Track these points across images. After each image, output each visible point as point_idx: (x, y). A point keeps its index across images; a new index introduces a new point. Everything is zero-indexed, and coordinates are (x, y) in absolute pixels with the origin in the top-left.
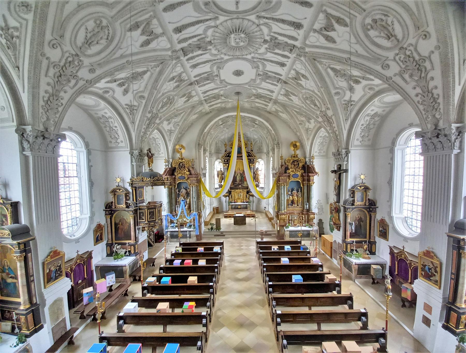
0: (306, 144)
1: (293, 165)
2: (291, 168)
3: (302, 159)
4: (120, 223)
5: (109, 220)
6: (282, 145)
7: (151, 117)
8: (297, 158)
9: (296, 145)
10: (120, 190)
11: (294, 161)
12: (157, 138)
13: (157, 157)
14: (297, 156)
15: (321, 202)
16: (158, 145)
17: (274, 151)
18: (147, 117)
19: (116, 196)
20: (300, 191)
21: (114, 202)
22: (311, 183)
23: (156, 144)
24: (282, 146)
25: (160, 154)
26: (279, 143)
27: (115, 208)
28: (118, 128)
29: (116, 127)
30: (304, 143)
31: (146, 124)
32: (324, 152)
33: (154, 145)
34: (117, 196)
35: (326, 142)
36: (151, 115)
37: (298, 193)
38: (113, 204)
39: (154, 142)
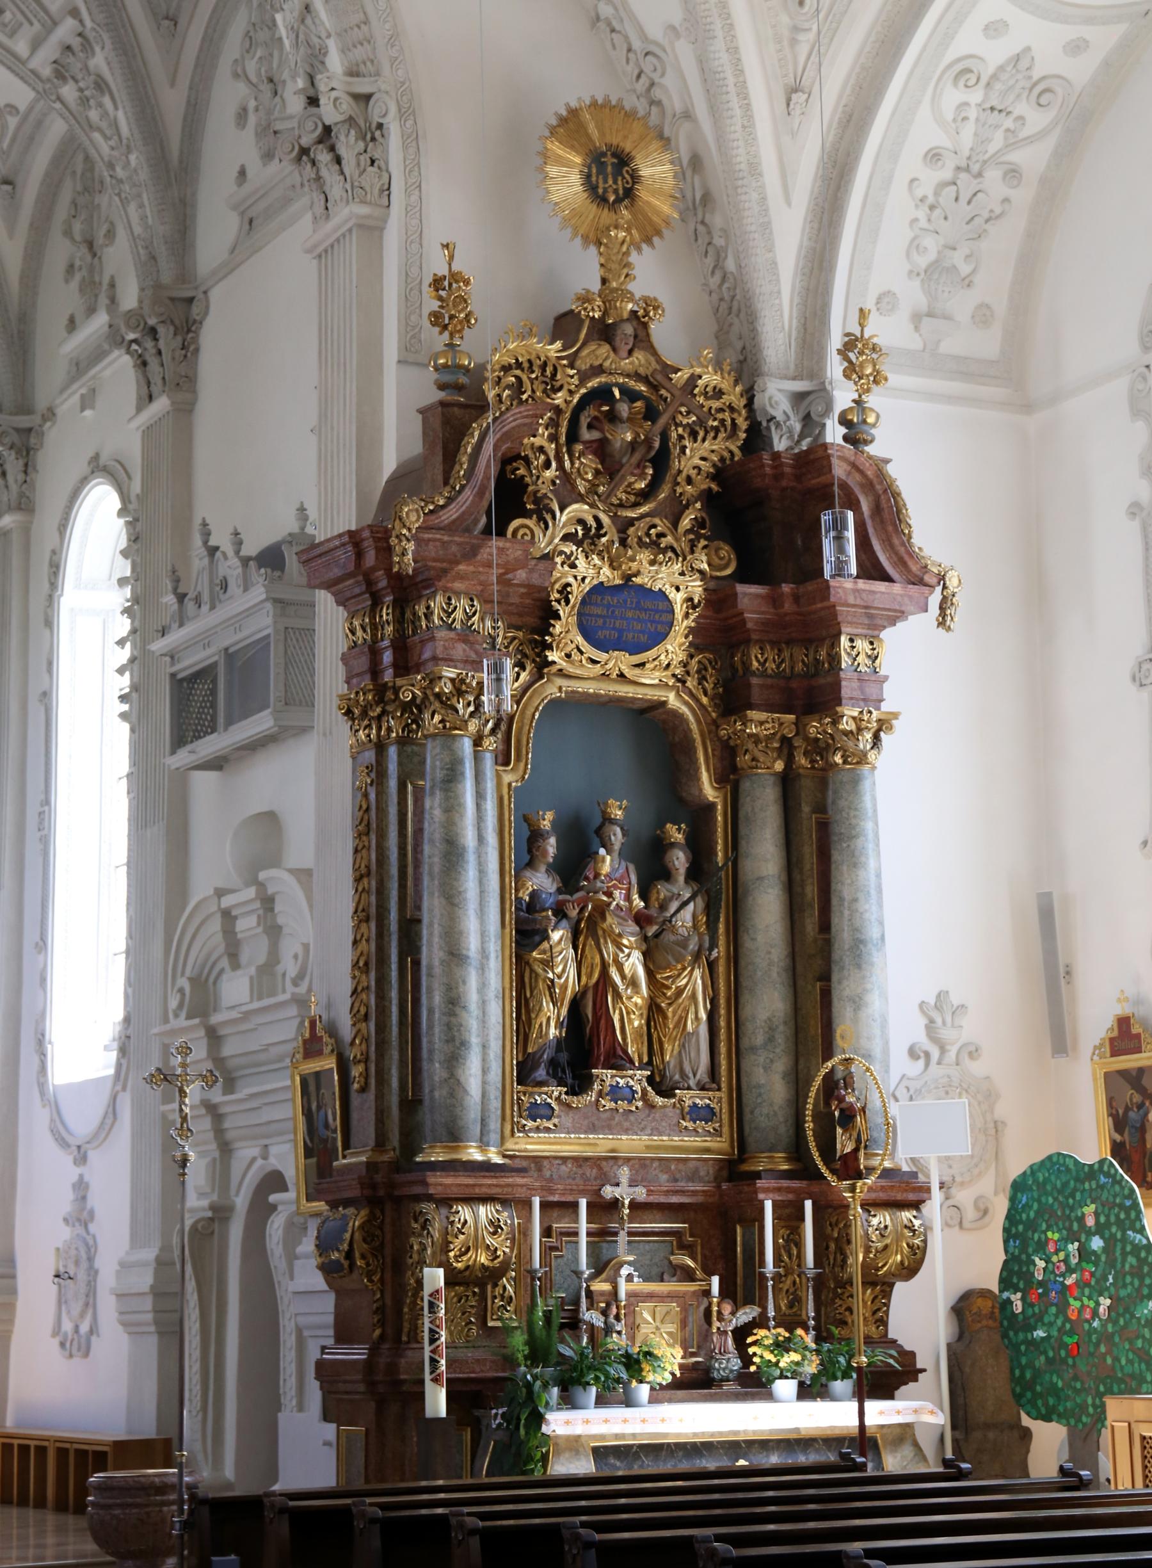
0: (755, 169)
1: (589, 462)
2: (567, 493)
3: (710, 378)
6: (413, 139)
8: (639, 357)
9: (623, 160)
11: (602, 394)
14: (640, 321)
15: (969, 1029)
17: (189, 348)
20: (679, 860)
22: (849, 712)
24: (414, 167)
26: (386, 109)
30: (741, 156)
32: (983, 315)
35: (1013, 174)
37: (662, 890)
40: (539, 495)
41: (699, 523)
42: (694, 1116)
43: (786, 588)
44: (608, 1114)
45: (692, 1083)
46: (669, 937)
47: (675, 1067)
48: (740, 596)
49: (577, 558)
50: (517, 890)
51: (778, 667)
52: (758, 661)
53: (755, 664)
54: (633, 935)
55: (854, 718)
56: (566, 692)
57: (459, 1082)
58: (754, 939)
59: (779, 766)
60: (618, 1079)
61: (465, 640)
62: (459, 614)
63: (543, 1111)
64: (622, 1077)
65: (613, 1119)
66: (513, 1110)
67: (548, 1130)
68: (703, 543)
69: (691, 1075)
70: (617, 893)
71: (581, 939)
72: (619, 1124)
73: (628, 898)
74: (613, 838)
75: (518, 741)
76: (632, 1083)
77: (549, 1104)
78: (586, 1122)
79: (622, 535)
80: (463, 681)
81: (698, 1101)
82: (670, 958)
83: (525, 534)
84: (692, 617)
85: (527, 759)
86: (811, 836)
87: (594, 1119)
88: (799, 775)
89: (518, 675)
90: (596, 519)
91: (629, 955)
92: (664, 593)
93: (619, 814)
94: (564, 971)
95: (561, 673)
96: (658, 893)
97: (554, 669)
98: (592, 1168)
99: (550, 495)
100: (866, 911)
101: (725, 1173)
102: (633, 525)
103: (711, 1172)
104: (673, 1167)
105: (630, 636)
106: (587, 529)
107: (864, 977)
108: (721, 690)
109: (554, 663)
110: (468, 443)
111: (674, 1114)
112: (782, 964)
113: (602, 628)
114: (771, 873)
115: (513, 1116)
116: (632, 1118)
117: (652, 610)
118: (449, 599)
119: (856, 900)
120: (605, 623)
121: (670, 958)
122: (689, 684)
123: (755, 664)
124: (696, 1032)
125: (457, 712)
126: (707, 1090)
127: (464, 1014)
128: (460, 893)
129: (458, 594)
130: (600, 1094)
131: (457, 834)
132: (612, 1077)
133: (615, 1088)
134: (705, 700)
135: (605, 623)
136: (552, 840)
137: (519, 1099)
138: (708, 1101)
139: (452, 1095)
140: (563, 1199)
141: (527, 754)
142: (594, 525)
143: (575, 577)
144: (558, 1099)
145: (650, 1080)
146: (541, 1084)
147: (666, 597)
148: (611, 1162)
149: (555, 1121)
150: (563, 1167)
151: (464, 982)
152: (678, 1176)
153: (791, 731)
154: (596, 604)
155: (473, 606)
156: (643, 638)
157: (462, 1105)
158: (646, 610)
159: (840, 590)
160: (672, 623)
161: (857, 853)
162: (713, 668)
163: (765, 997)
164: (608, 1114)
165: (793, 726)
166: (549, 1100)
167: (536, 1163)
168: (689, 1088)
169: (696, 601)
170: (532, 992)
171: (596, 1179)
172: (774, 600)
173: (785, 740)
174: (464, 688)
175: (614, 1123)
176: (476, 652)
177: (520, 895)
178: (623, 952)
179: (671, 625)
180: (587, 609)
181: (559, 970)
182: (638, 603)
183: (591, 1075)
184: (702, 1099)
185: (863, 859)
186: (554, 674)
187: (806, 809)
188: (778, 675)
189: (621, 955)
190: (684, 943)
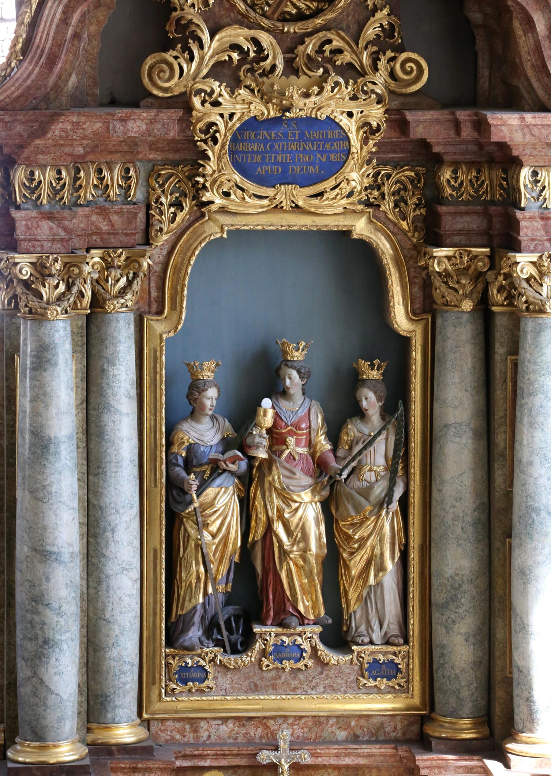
40: (183, 22)
41: (389, 31)
42: (374, 673)
43: (462, 115)
44: (273, 673)
45: (377, 636)
46: (356, 483)
47: (361, 617)
48: (412, 125)
49: (221, 95)
50: (169, 444)
51: (476, 191)
52: (453, 188)
53: (449, 191)
54: (304, 488)
55: (533, 263)
56: (229, 232)
57: (42, 682)
58: (440, 491)
59: (467, 305)
60: (285, 638)
61: (50, 216)
62: (45, 190)
63: (194, 675)
64: (289, 636)
65: (280, 677)
66: (161, 675)
67: (201, 692)
68: (390, 54)
69: (376, 627)
70: (291, 440)
71: (252, 489)
72: (286, 683)
73: (310, 444)
74: (288, 382)
75: (174, 288)
76: (299, 640)
77: (203, 667)
78: (247, 682)
79: (289, 55)
80: (44, 266)
81: (381, 658)
82: (350, 507)
83: (163, 71)
84: (371, 142)
85: (182, 307)
86: (505, 380)
87: (255, 679)
88: (493, 313)
89: (175, 215)
90: (256, 42)
91: (297, 510)
92: (333, 121)
93: (297, 356)
94: (219, 529)
95: (223, 210)
96: (347, 434)
97: (213, 207)
98: (257, 727)
99: (195, 21)
100: (541, 476)
101: (415, 728)
102: (303, 43)
103: (399, 727)
104: (353, 723)
105: (297, 169)
106: (243, 53)
107: (535, 549)
108: (423, 211)
109: (212, 202)
110: (27, 12)
111: (352, 673)
112: (469, 519)
113: (261, 164)
114: (458, 420)
115: (161, 681)
116: (301, 676)
117: (320, 140)
118: (32, 173)
119: (531, 463)
120: (263, 158)
121: (350, 507)
122: (383, 208)
123: (449, 191)
124: (379, 584)
125: (41, 297)
126: (393, 644)
127: (48, 612)
128: (45, 487)
129: (43, 167)
130: (264, 653)
131: (42, 426)
132: (277, 635)
133: (280, 648)
134: (404, 224)
135: (263, 158)
136: (212, 393)
137: (168, 665)
138: (391, 657)
139: (35, 693)
140: (216, 764)
141: (182, 301)
142: (253, 48)
143: (222, 115)
144: (213, 660)
145: (323, 637)
146: (190, 649)
147: (338, 124)
148: (280, 721)
149: (209, 682)
150: (223, 728)
151: (48, 579)
152: (359, 732)
153: (484, 265)
154: (250, 141)
155: (60, 179)
156: (315, 170)
157: (45, 705)
158: (312, 142)
159: (503, 128)
160: (349, 150)
161: (534, 412)
162: (415, 187)
163: (448, 554)
164: (273, 673)
165: (486, 260)
166: (202, 663)
167: (192, 725)
168: (372, 643)
169: (374, 124)
170: (184, 552)
171: (261, 738)
172: (457, 125)
173: (479, 276)
174: (47, 272)
175: (278, 682)
176: (65, 229)
177: (175, 449)
178: (289, 506)
179: (348, 152)
180: (240, 147)
181: (214, 528)
182: (302, 135)
183: (255, 634)
184: (385, 653)
185: (540, 419)
186: (216, 212)
187: (500, 350)
188: (476, 199)
189: (287, 510)
190: (366, 493)
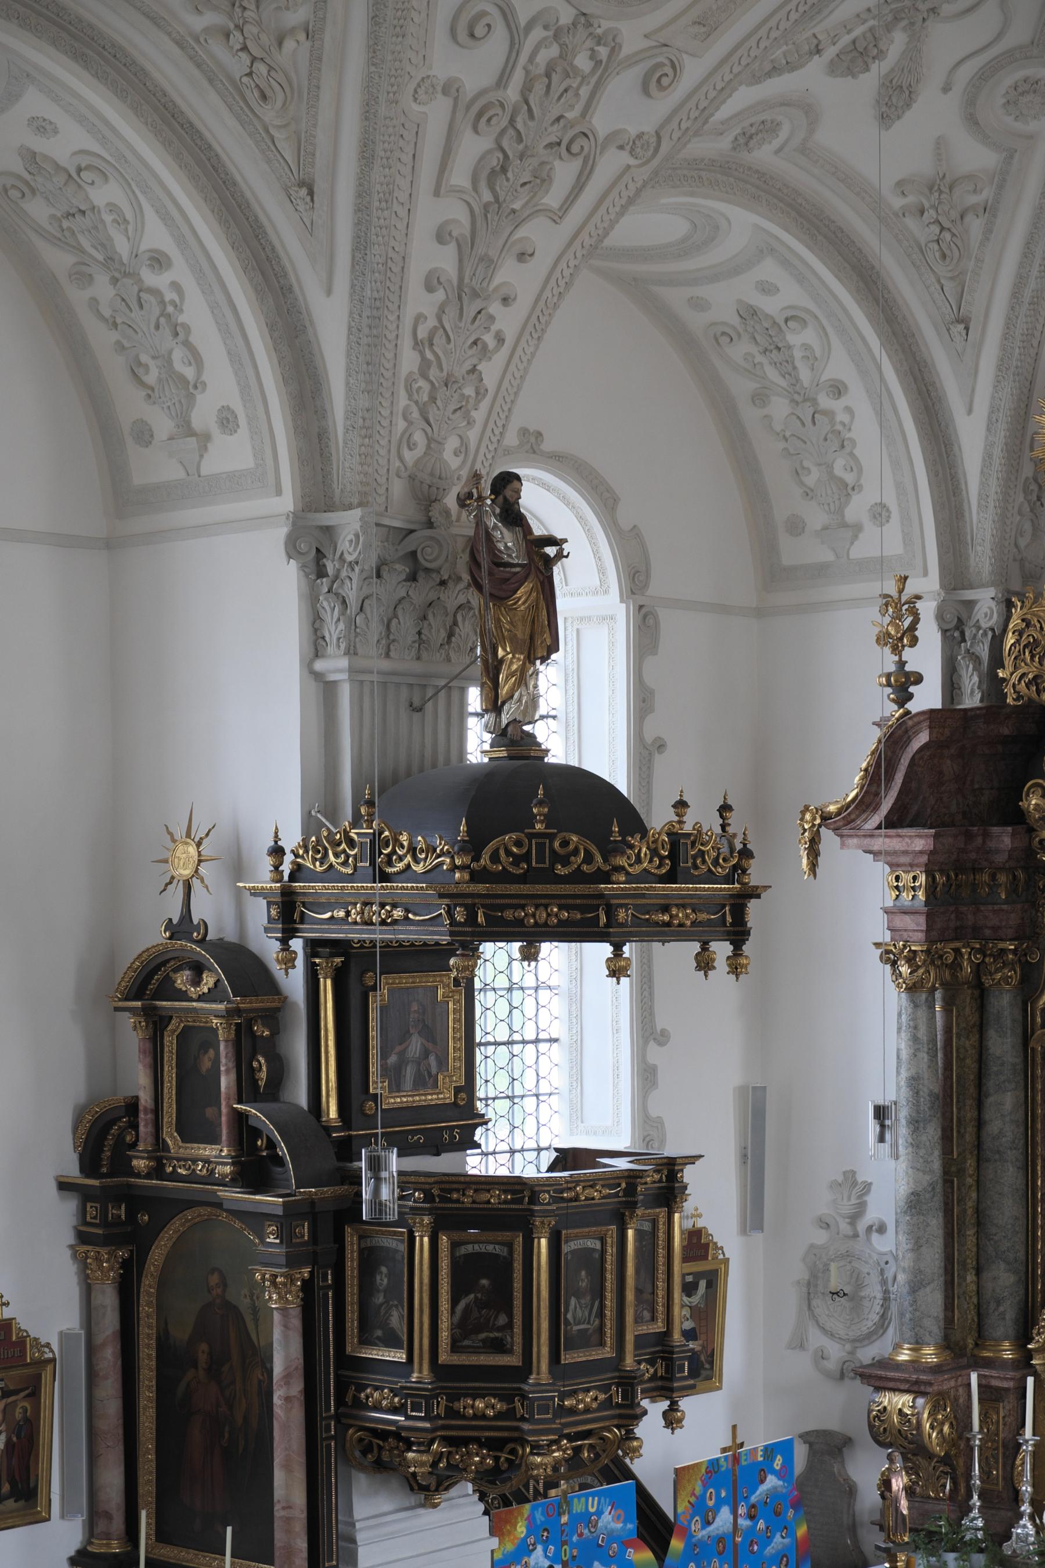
4: (203, 1358)
5: (108, 1299)
7: (502, 81)
10: (198, 969)
12: (794, 318)
13: (820, 572)
16: (825, 402)
18: (450, 88)
19: (170, 1042)
21: (145, 1099)
23: (800, 396)
25: (857, 529)
27: (157, 1171)
28: (180, 271)
29: (159, 261)
31: (460, 177)
33: (780, 408)
34: (184, 1036)
36: (496, 46)
38: (145, 1129)
39: (772, 374)
